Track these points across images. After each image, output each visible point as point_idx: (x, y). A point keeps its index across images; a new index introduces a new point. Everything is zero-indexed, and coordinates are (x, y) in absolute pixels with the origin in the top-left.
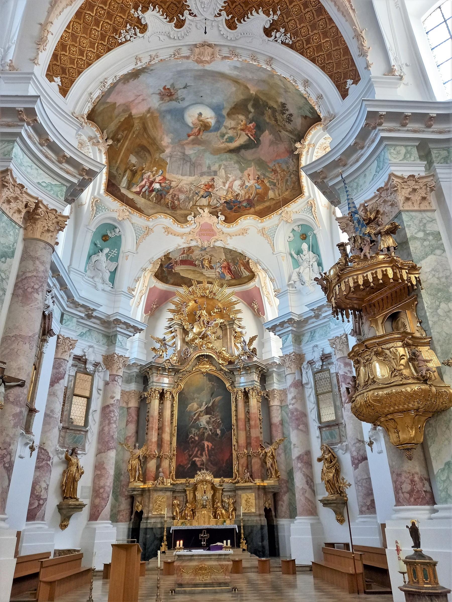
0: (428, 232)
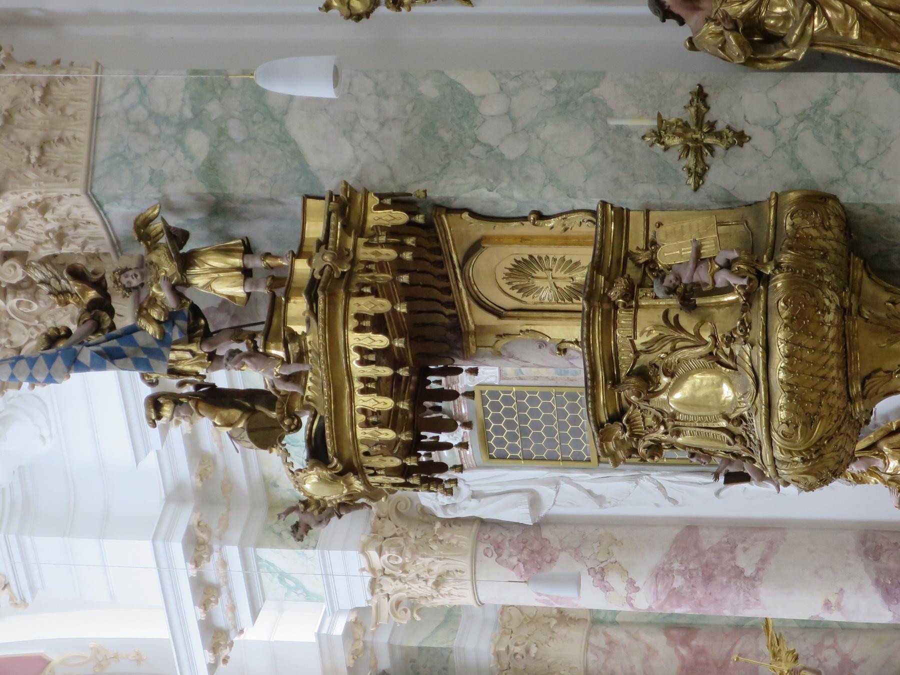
0: (188, 113)
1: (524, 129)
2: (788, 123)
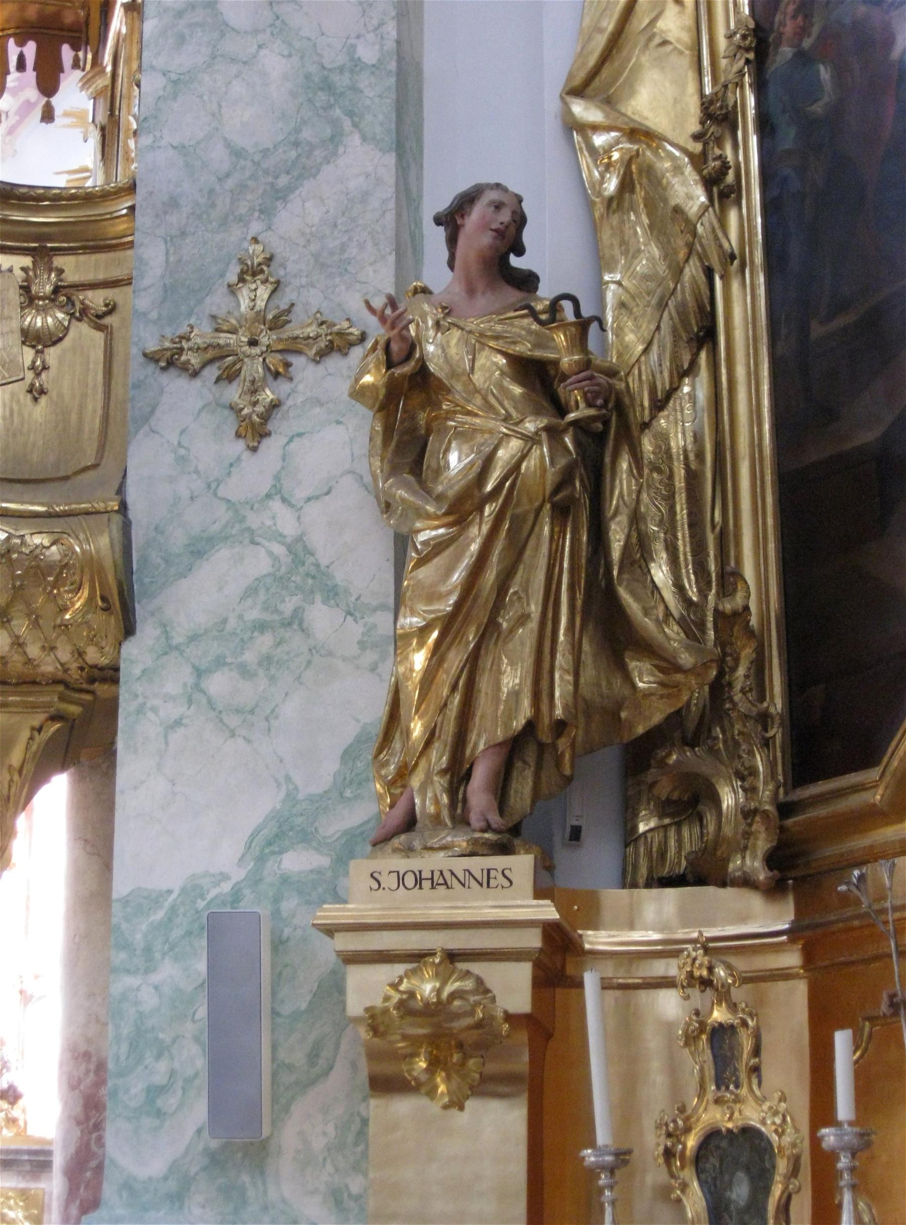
1: (278, 18)
2: (288, 525)
